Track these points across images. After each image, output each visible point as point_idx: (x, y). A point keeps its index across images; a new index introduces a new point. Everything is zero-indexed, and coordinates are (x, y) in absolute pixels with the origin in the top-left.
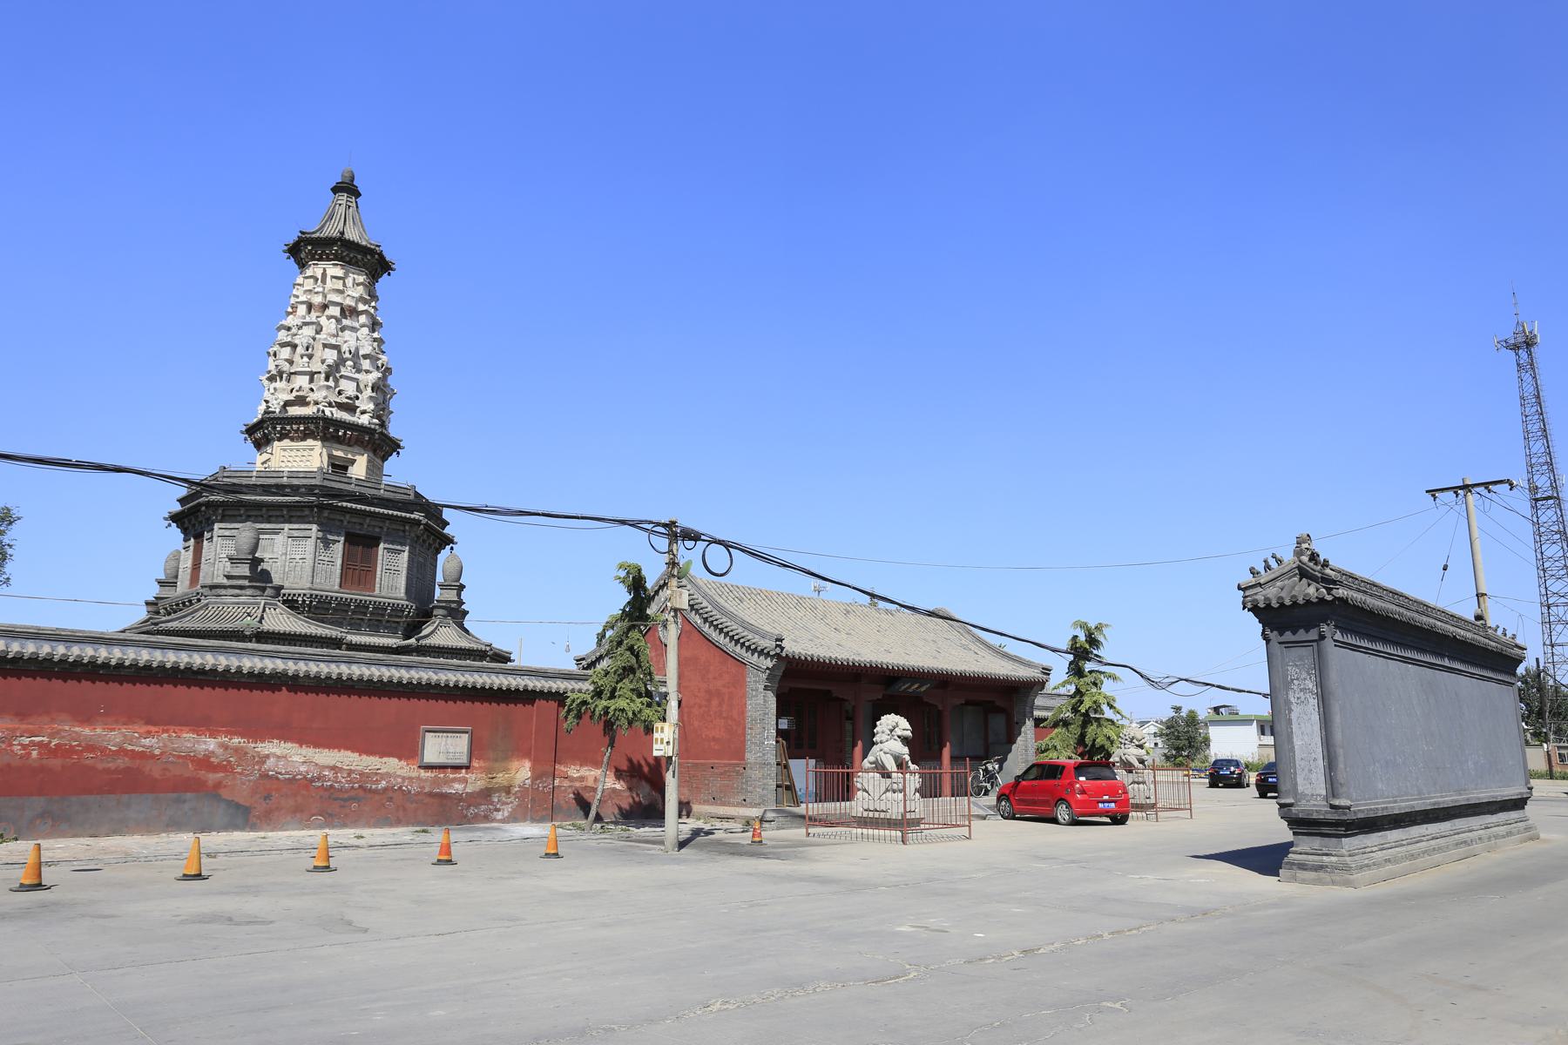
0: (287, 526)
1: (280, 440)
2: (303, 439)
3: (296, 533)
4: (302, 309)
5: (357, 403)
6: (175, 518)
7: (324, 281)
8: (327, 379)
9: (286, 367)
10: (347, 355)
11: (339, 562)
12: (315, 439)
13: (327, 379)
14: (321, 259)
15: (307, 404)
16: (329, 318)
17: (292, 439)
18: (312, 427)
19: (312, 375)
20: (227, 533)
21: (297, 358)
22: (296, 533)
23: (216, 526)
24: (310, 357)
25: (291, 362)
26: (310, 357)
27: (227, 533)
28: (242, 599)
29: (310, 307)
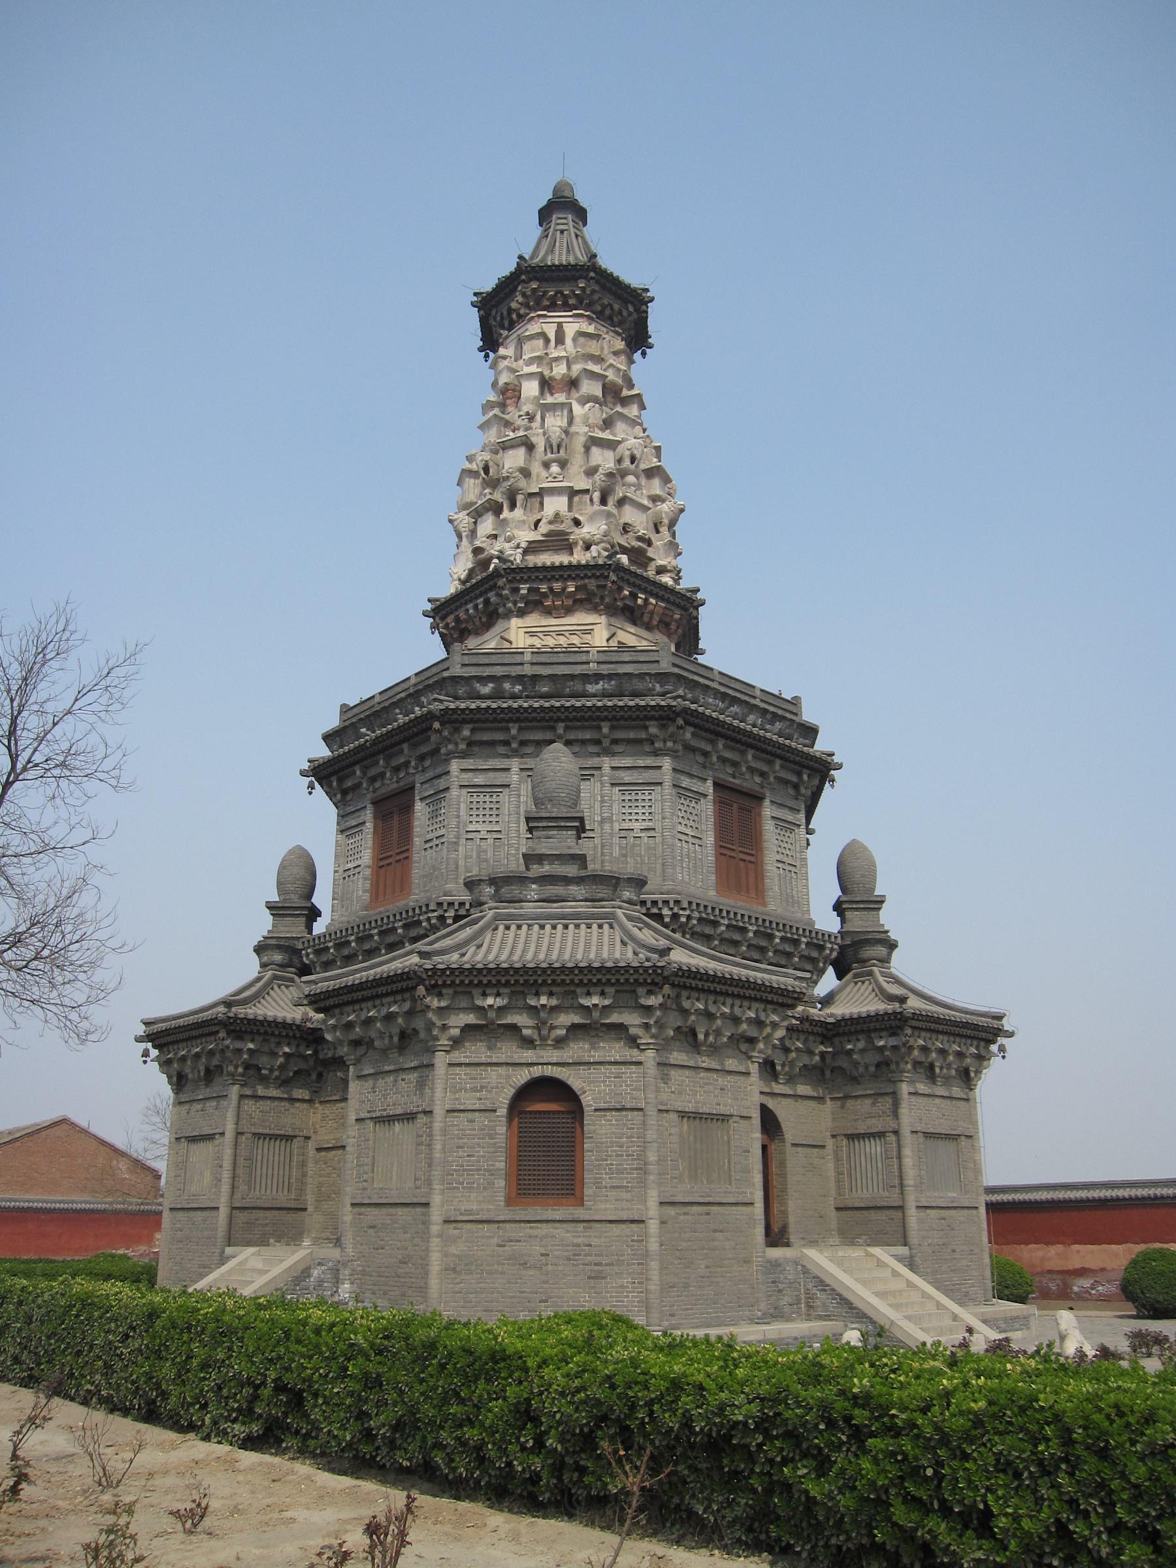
0: (607, 763)
1: (521, 613)
2: (569, 611)
3: (627, 777)
4: (531, 389)
5: (650, 553)
6: (323, 774)
7: (560, 340)
8: (603, 501)
9: (522, 483)
10: (627, 463)
11: (710, 839)
12: (595, 609)
13: (603, 501)
14: (553, 307)
15: (570, 548)
16: (584, 401)
17: (548, 612)
18: (592, 584)
19: (572, 493)
20: (479, 779)
21: (536, 468)
22: (627, 777)
23: (455, 766)
24: (563, 464)
25: (526, 473)
26: (563, 464)
27: (479, 779)
28: (569, 908)
29: (546, 384)
